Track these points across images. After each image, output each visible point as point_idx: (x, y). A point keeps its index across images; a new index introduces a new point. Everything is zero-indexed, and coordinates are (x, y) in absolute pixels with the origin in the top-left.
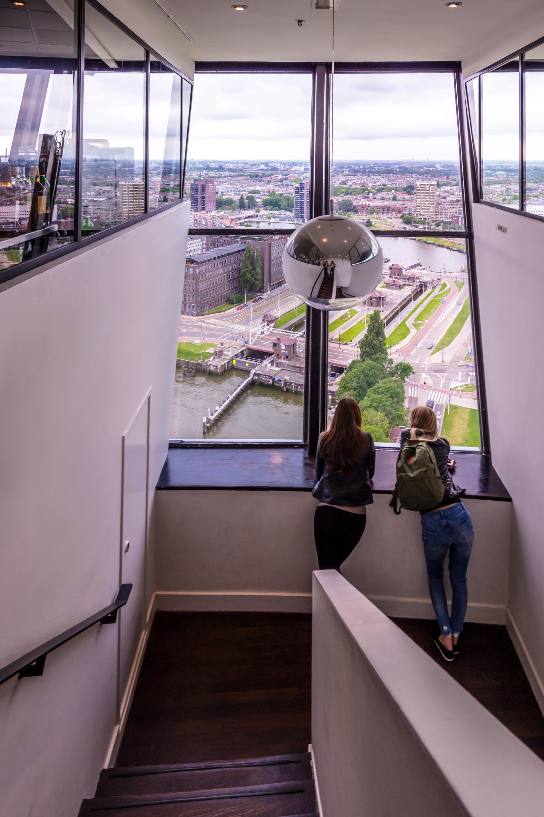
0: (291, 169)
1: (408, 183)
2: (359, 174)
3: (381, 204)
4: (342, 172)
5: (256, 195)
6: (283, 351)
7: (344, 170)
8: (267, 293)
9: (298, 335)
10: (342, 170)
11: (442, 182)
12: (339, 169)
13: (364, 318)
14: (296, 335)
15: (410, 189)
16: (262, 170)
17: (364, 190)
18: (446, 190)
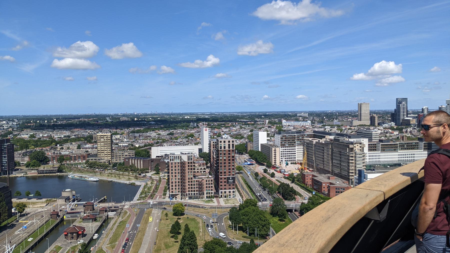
2: (45, 128)
3: (68, 153)
13: (69, 250)
15: (89, 139)
18: (117, 138)
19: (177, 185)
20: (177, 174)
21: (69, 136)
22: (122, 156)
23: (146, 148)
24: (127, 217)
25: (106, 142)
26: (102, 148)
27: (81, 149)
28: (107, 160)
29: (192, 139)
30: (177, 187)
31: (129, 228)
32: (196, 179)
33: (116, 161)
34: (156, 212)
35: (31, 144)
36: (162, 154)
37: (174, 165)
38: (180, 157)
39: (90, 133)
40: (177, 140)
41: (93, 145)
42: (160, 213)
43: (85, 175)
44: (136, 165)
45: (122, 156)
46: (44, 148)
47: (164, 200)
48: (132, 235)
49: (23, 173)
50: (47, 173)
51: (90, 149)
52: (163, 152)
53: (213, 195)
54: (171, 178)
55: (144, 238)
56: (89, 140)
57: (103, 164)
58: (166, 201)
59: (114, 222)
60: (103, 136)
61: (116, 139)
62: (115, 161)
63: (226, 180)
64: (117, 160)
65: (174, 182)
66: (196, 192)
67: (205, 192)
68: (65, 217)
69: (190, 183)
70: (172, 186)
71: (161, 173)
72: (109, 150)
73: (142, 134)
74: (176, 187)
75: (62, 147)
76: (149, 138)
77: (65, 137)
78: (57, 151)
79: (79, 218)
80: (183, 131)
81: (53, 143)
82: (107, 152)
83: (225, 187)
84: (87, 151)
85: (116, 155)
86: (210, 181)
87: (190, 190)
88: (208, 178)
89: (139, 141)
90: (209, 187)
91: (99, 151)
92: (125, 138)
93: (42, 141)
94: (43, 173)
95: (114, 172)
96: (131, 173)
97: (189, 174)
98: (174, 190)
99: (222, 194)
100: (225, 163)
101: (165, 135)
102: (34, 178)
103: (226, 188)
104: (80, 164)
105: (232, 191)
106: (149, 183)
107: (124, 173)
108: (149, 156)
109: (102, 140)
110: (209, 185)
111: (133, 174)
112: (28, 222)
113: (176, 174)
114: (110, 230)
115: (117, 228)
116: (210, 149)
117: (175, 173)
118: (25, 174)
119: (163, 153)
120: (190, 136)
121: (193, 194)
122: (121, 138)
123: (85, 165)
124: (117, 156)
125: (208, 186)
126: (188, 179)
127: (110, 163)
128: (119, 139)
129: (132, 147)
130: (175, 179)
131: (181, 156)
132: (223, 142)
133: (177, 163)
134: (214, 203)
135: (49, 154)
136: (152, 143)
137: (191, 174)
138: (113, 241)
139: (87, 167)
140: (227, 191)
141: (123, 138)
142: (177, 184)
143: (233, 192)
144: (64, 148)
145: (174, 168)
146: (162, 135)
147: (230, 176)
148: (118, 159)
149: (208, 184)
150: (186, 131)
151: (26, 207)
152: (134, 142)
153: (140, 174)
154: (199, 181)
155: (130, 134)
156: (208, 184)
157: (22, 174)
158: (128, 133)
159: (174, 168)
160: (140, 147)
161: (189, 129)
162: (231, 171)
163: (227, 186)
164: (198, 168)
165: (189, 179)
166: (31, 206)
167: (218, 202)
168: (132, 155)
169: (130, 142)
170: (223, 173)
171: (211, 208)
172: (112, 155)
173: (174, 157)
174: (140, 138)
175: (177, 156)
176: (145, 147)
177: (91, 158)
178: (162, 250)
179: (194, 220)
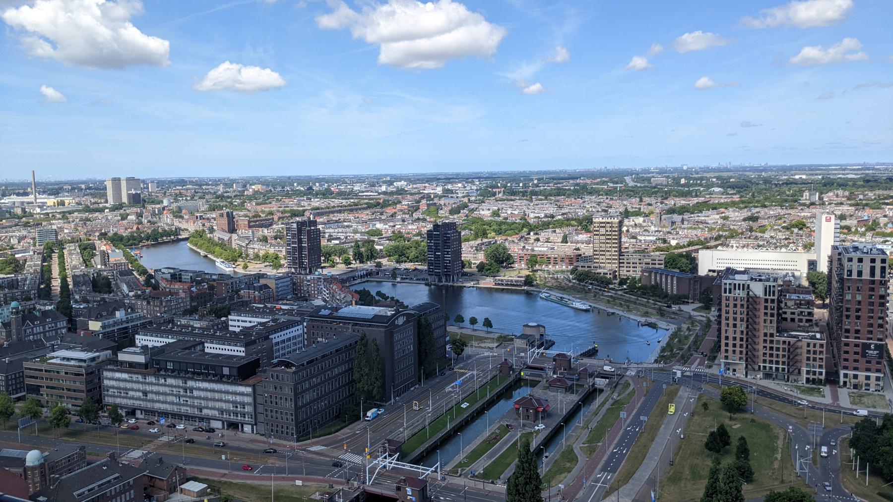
0: (424, 192)
1: (585, 211)
2: (518, 198)
3: (545, 249)
4: (494, 194)
5: (376, 239)
6: (409, 497)
7: (497, 190)
8: (390, 402)
9: (429, 472)
10: (494, 190)
11: (632, 208)
12: (490, 190)
14: (428, 472)
16: (385, 193)
17: (523, 227)
19: (738, 345)
20: (738, 323)
21: (552, 216)
22: (640, 263)
23: (691, 248)
24: (629, 394)
25: (609, 235)
26: (601, 247)
27: (569, 244)
28: (609, 270)
29: (801, 232)
30: (738, 349)
31: (626, 420)
32: (784, 336)
33: (628, 274)
34: (685, 394)
35: (492, 228)
36: (721, 265)
37: (731, 303)
38: (746, 286)
39: (590, 210)
40: (764, 232)
41: (590, 237)
42: (694, 398)
43: (569, 295)
44: (664, 285)
45: (640, 263)
46: (509, 238)
47: (707, 370)
48: (630, 435)
49: (472, 280)
50: (507, 285)
51: (583, 243)
52: (723, 261)
53: (823, 377)
54: (723, 328)
55: (653, 446)
56: (586, 225)
57: (601, 278)
58: (713, 375)
59: (603, 400)
60: (604, 223)
61: (636, 225)
62: (625, 273)
63: (859, 349)
64: (629, 271)
65: (731, 338)
66: (781, 366)
67: (804, 369)
68: (522, 374)
69: (768, 345)
70: (727, 345)
71: (713, 309)
72: (615, 251)
73: (690, 216)
74: (734, 349)
75: (537, 236)
76: (701, 226)
77: (546, 216)
78: (529, 244)
79: (545, 380)
80: (782, 212)
81: (525, 229)
82: (610, 255)
83: (856, 365)
84: (578, 249)
85: (628, 261)
86: (818, 346)
87: (768, 358)
88: (813, 337)
89: (680, 233)
90: (815, 360)
91: (596, 251)
92: (652, 223)
93: (508, 224)
94: (502, 285)
95: (621, 295)
96: (653, 302)
97: (766, 324)
98: (730, 353)
99: (847, 380)
100: (858, 310)
101: (738, 221)
102: (490, 290)
103: (859, 367)
104: (563, 272)
105: (873, 375)
106: (685, 326)
107: (638, 300)
108: (695, 268)
109: (603, 231)
110: (814, 354)
111: (656, 304)
112: (466, 373)
113: (735, 322)
114: (593, 415)
115: (606, 414)
116: (830, 271)
117: (735, 319)
118: (476, 284)
119: (723, 265)
120: (796, 226)
121: (774, 369)
122: (644, 224)
123: (571, 277)
124: (630, 263)
125: (812, 356)
126: (763, 335)
127: (615, 277)
128: (640, 226)
129: (662, 245)
130: (734, 331)
131: (749, 285)
132: (855, 261)
133: (739, 300)
134: (824, 396)
135: (515, 248)
136: (706, 239)
137: (772, 325)
138: (596, 436)
139: (573, 279)
140: (862, 374)
141: (650, 224)
142: (738, 342)
143: (878, 379)
144: (541, 240)
145: (731, 309)
146: (730, 221)
147: (871, 341)
148: (631, 269)
149: (812, 352)
150: (790, 211)
151: (466, 346)
152: (669, 233)
153: (669, 307)
154: (789, 342)
155: (664, 217)
156: (812, 352)
157: (472, 283)
158: (659, 215)
159: (731, 309)
160: (678, 246)
161: (797, 208)
162: (875, 329)
163: (862, 363)
164: (793, 311)
165: (765, 335)
166: (475, 343)
167: (835, 397)
168: (659, 264)
169: (661, 233)
170: (852, 331)
171: (813, 407)
172: (621, 261)
173: (733, 285)
174: (683, 226)
175: (739, 285)
176: (689, 246)
177: (582, 264)
178: (683, 482)
179: (766, 427)
